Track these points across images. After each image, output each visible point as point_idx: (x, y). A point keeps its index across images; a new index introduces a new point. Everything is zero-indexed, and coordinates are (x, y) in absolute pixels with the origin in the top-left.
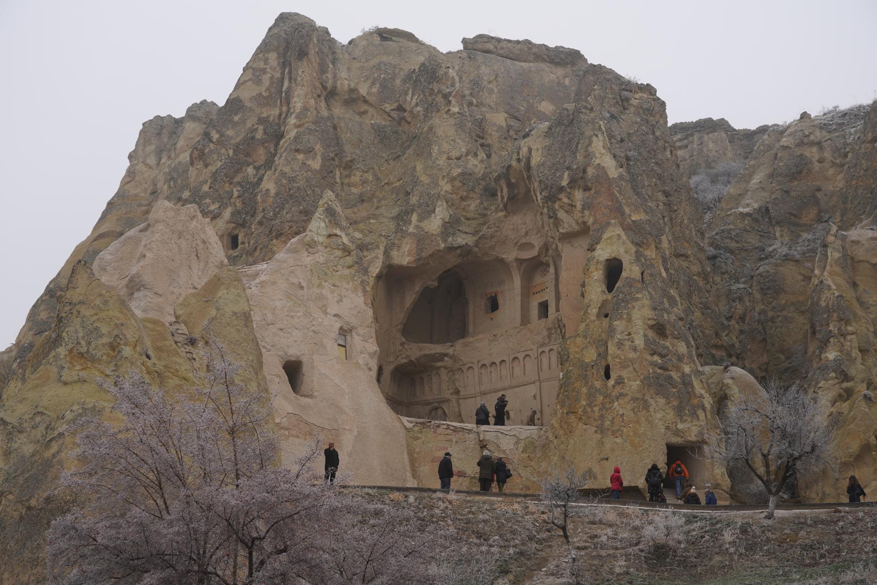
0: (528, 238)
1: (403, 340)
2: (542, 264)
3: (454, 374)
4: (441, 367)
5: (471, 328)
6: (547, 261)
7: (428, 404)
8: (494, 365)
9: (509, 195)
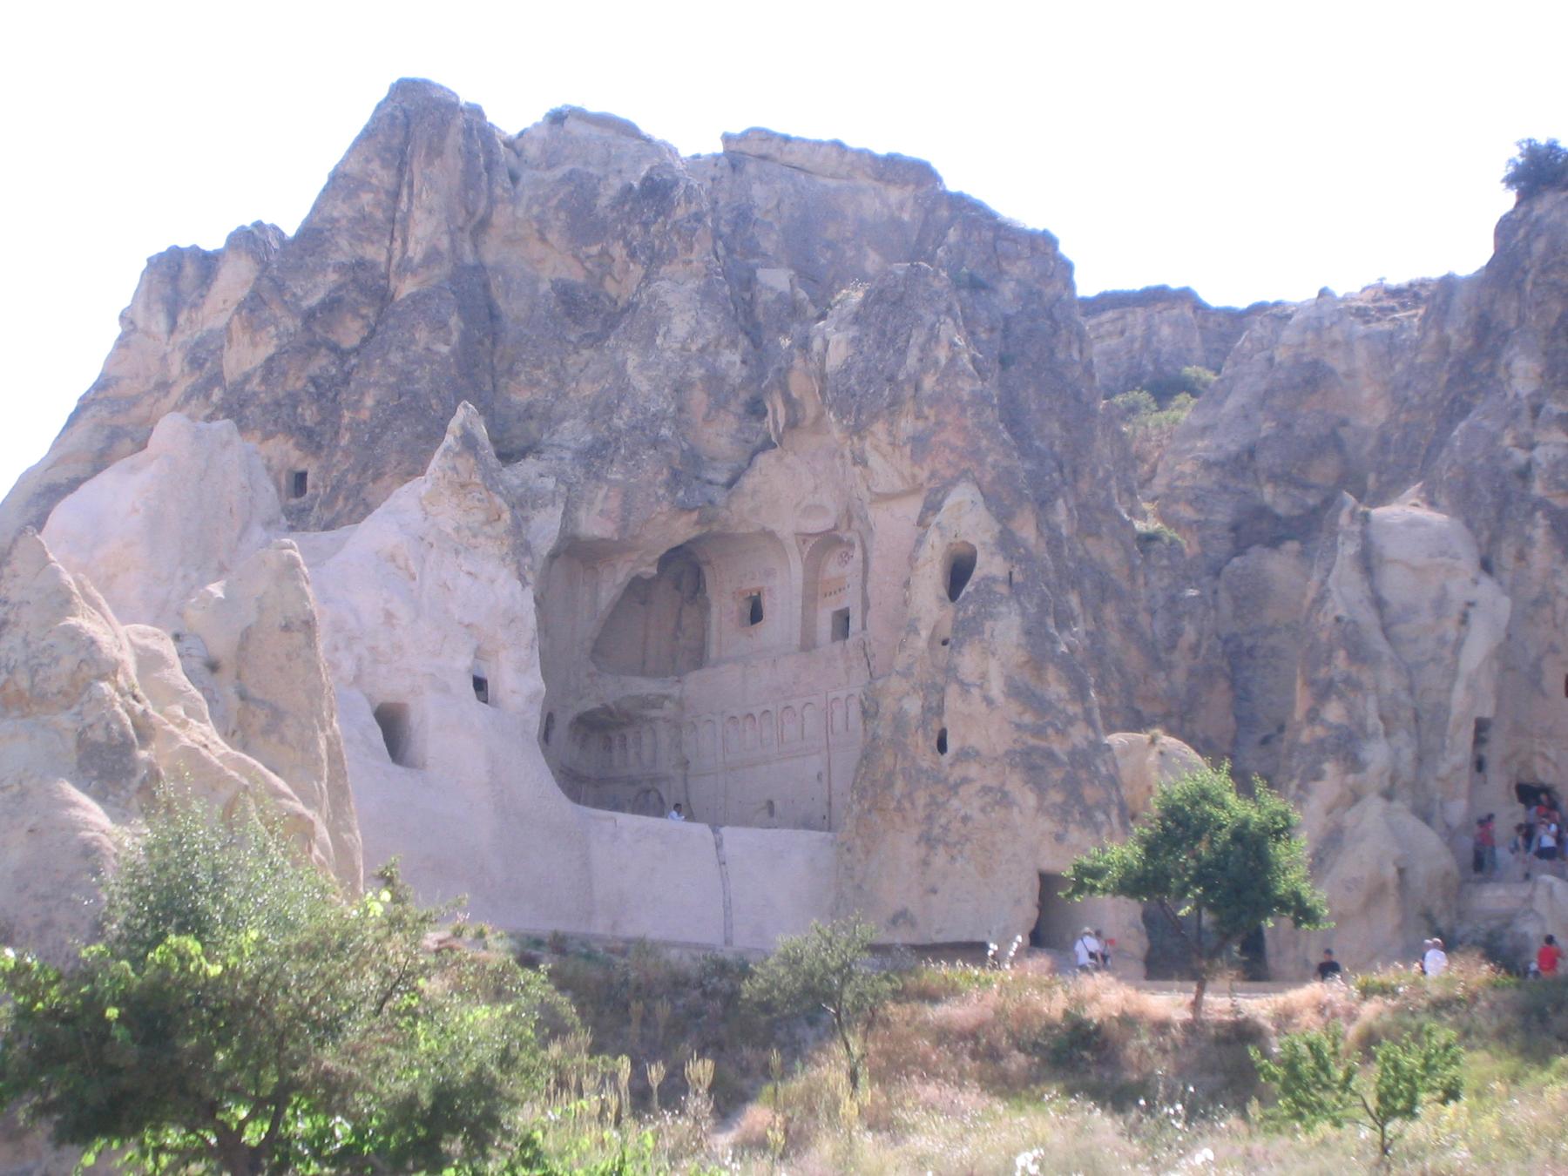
1: (593, 668)
2: (839, 541)
5: (713, 651)
9: (787, 420)
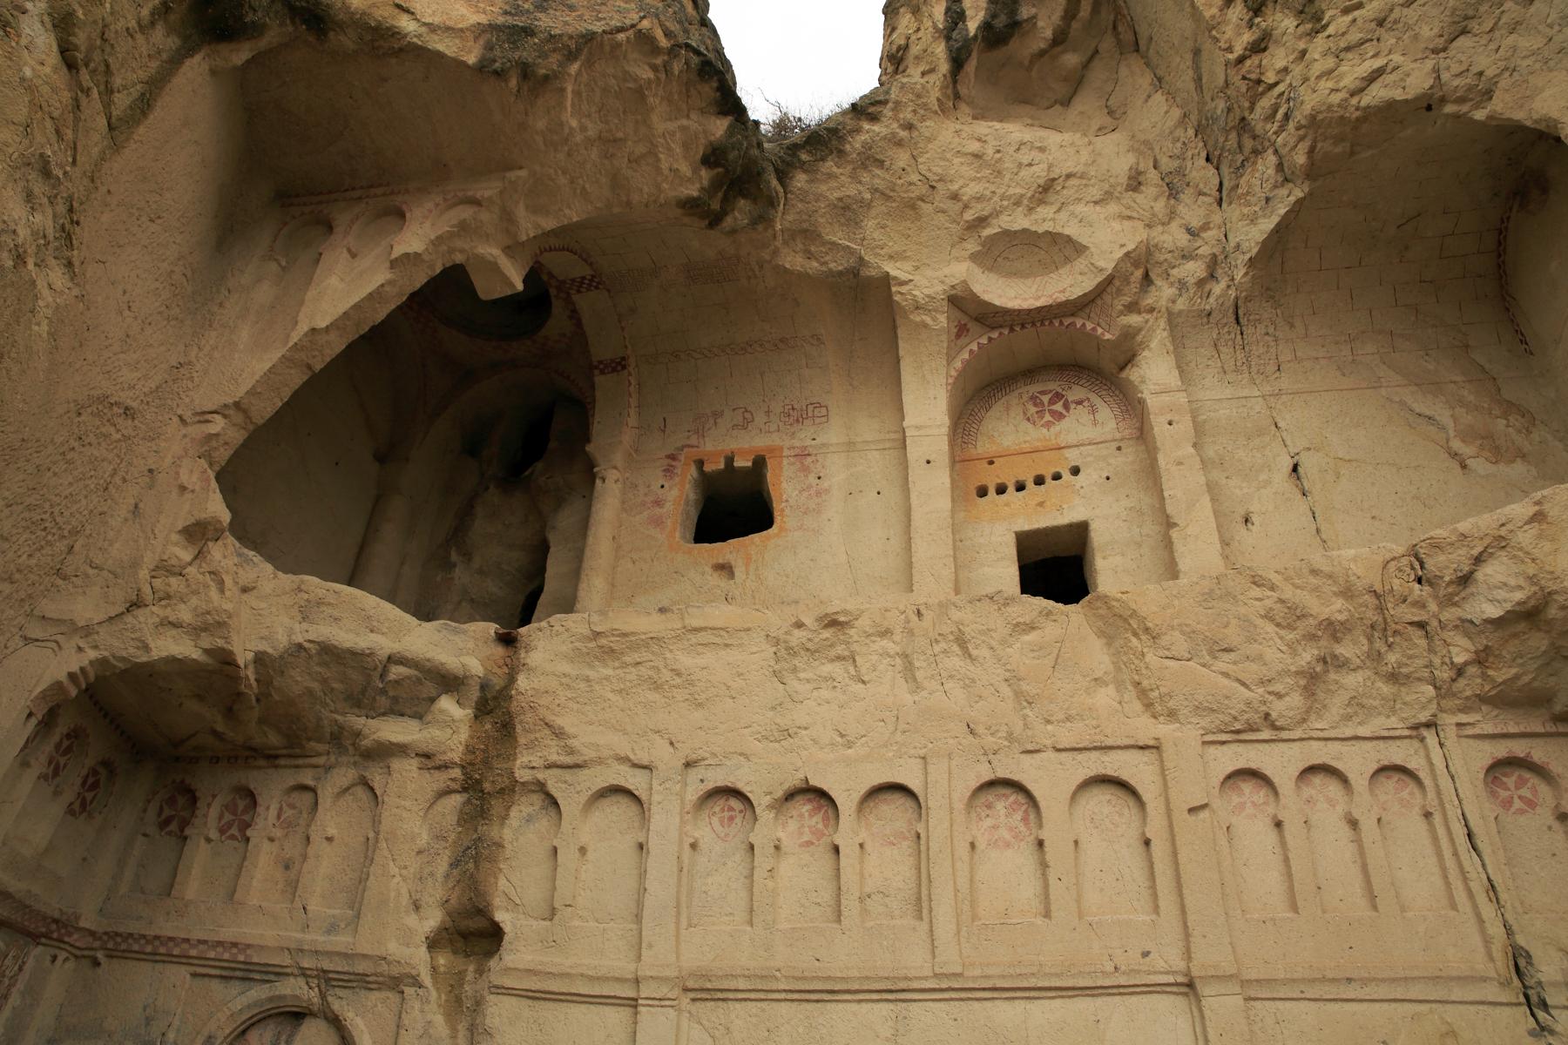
0: (1044, 212)
1: (217, 508)
4: (401, 750)
6: (1129, 335)
7: (245, 972)
8: (803, 807)
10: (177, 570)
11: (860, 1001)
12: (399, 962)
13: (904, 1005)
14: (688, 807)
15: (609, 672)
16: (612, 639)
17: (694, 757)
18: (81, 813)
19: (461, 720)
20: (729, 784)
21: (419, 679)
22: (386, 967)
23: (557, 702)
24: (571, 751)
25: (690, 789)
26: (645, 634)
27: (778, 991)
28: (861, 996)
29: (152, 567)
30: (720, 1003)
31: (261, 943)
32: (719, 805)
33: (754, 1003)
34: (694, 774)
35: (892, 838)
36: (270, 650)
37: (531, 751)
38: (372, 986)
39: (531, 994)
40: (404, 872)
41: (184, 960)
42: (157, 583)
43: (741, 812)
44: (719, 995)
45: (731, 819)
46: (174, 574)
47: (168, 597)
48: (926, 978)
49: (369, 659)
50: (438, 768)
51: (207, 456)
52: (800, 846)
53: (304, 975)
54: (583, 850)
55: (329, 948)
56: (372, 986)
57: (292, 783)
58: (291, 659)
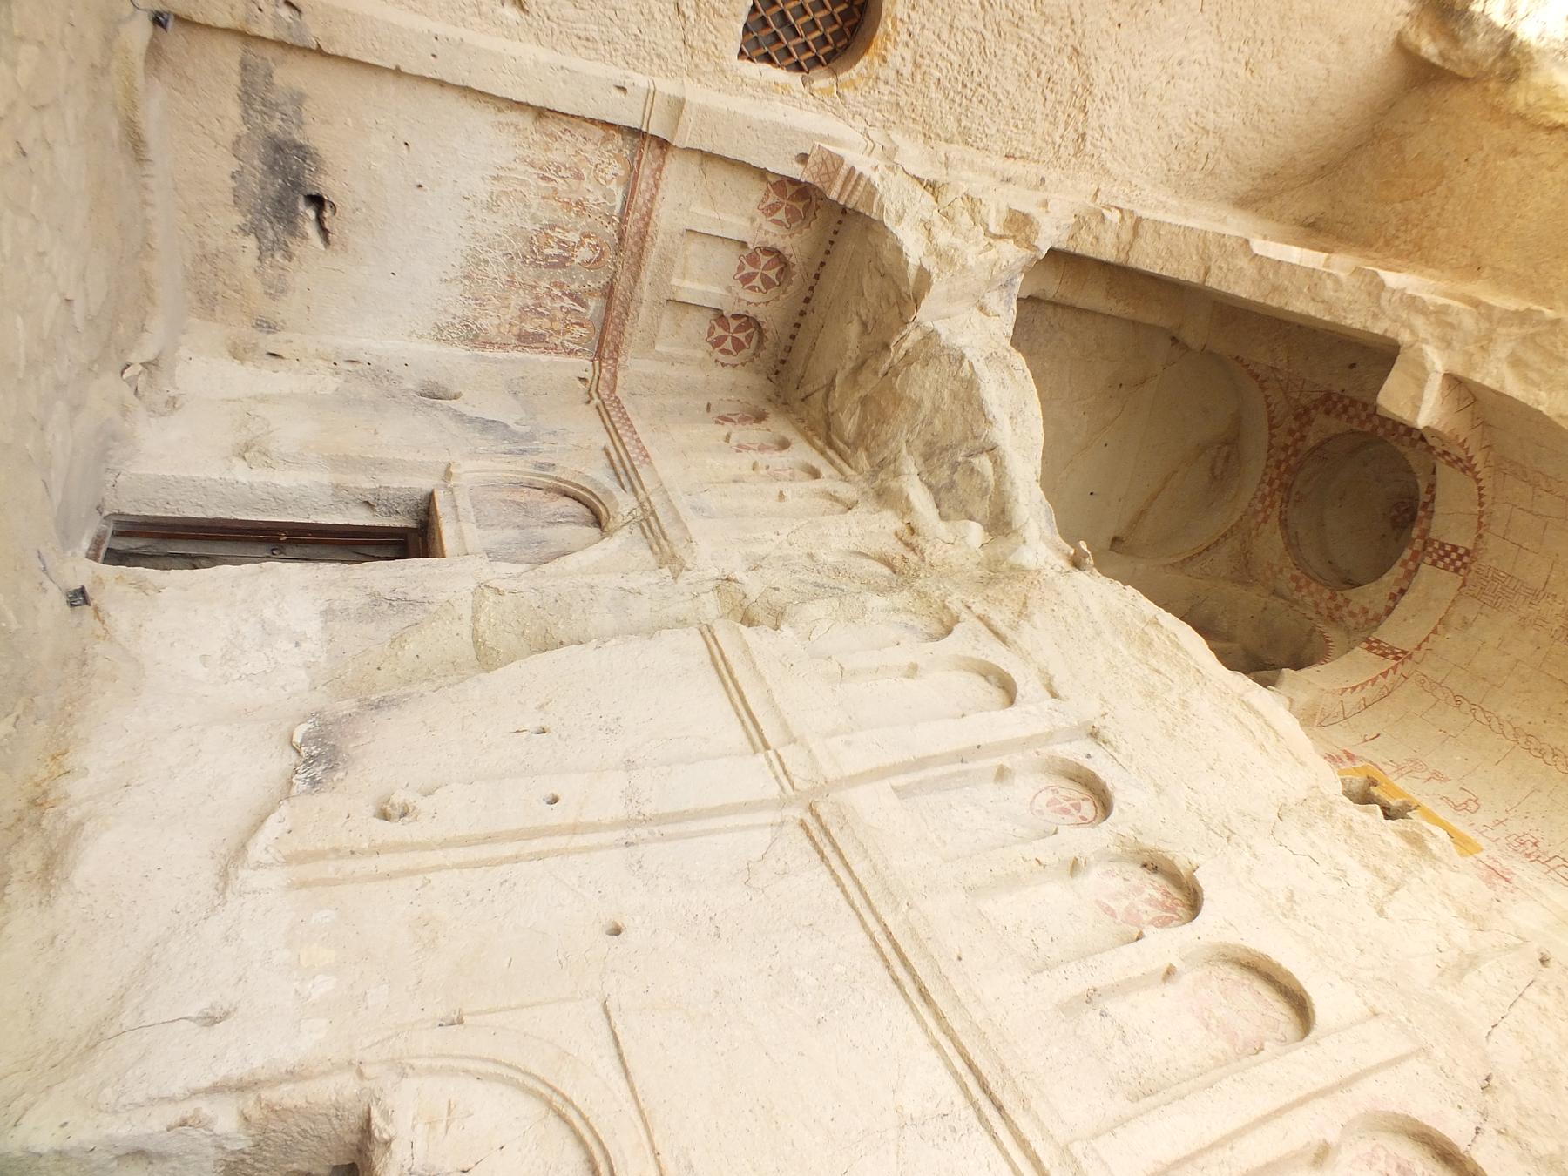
3: (881, 591)
7: (625, 472)
10: (978, 217)
11: (937, 1046)
12: (693, 552)
13: (975, 1122)
14: (1046, 751)
15: (1125, 653)
16: (1163, 637)
17: (1110, 737)
18: (711, 343)
19: (968, 546)
20: (1109, 786)
21: (987, 489)
22: (682, 546)
23: (1055, 608)
24: (1014, 627)
25: (1068, 746)
26: (1196, 662)
27: (879, 919)
28: (945, 1043)
29: (971, 194)
30: (818, 857)
31: (657, 469)
32: (1076, 792)
33: (841, 896)
34: (1088, 746)
35: (1213, 1021)
36: (943, 337)
37: (985, 602)
38: (655, 547)
39: (718, 657)
40: (786, 545)
41: (615, 438)
42: (959, 203)
43: (1082, 818)
44: (828, 850)
45: (1066, 811)
46: (973, 218)
47: (951, 220)
48: (1048, 1136)
49: (983, 425)
50: (907, 545)
51: (1081, 223)
52: (1097, 902)
53: (641, 505)
54: (913, 671)
55: (679, 507)
56: (655, 547)
57: (815, 465)
58: (944, 360)
